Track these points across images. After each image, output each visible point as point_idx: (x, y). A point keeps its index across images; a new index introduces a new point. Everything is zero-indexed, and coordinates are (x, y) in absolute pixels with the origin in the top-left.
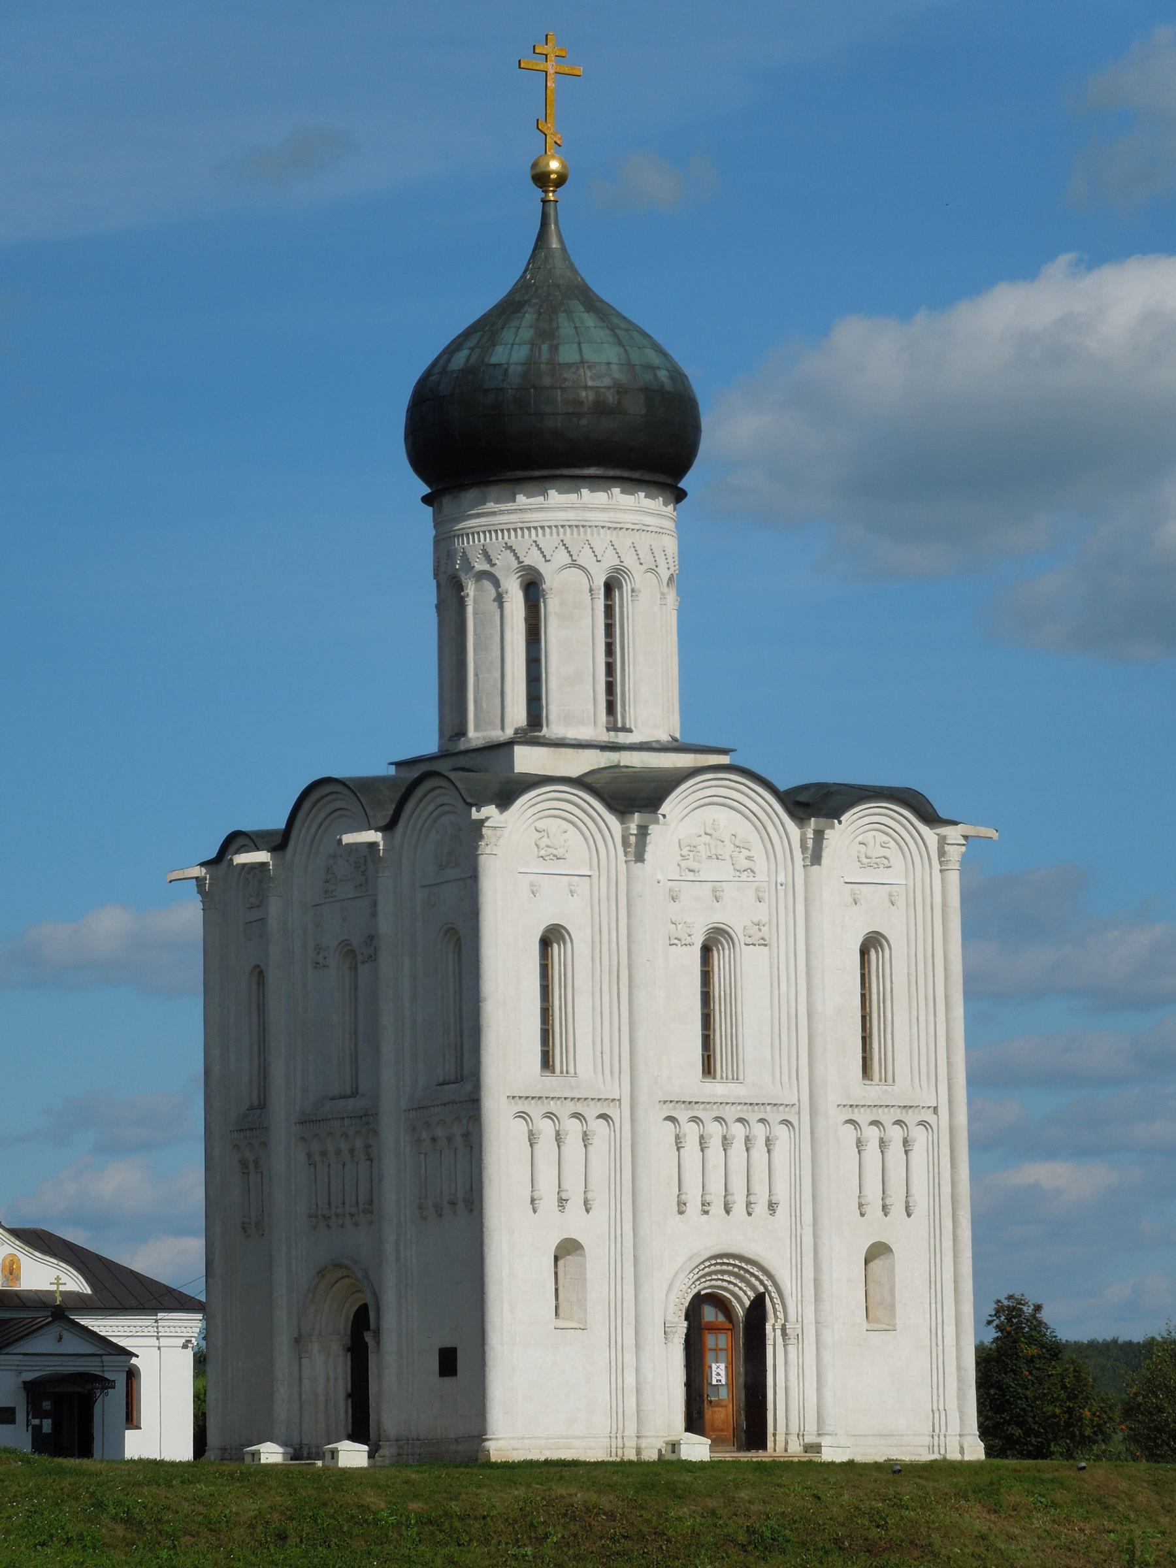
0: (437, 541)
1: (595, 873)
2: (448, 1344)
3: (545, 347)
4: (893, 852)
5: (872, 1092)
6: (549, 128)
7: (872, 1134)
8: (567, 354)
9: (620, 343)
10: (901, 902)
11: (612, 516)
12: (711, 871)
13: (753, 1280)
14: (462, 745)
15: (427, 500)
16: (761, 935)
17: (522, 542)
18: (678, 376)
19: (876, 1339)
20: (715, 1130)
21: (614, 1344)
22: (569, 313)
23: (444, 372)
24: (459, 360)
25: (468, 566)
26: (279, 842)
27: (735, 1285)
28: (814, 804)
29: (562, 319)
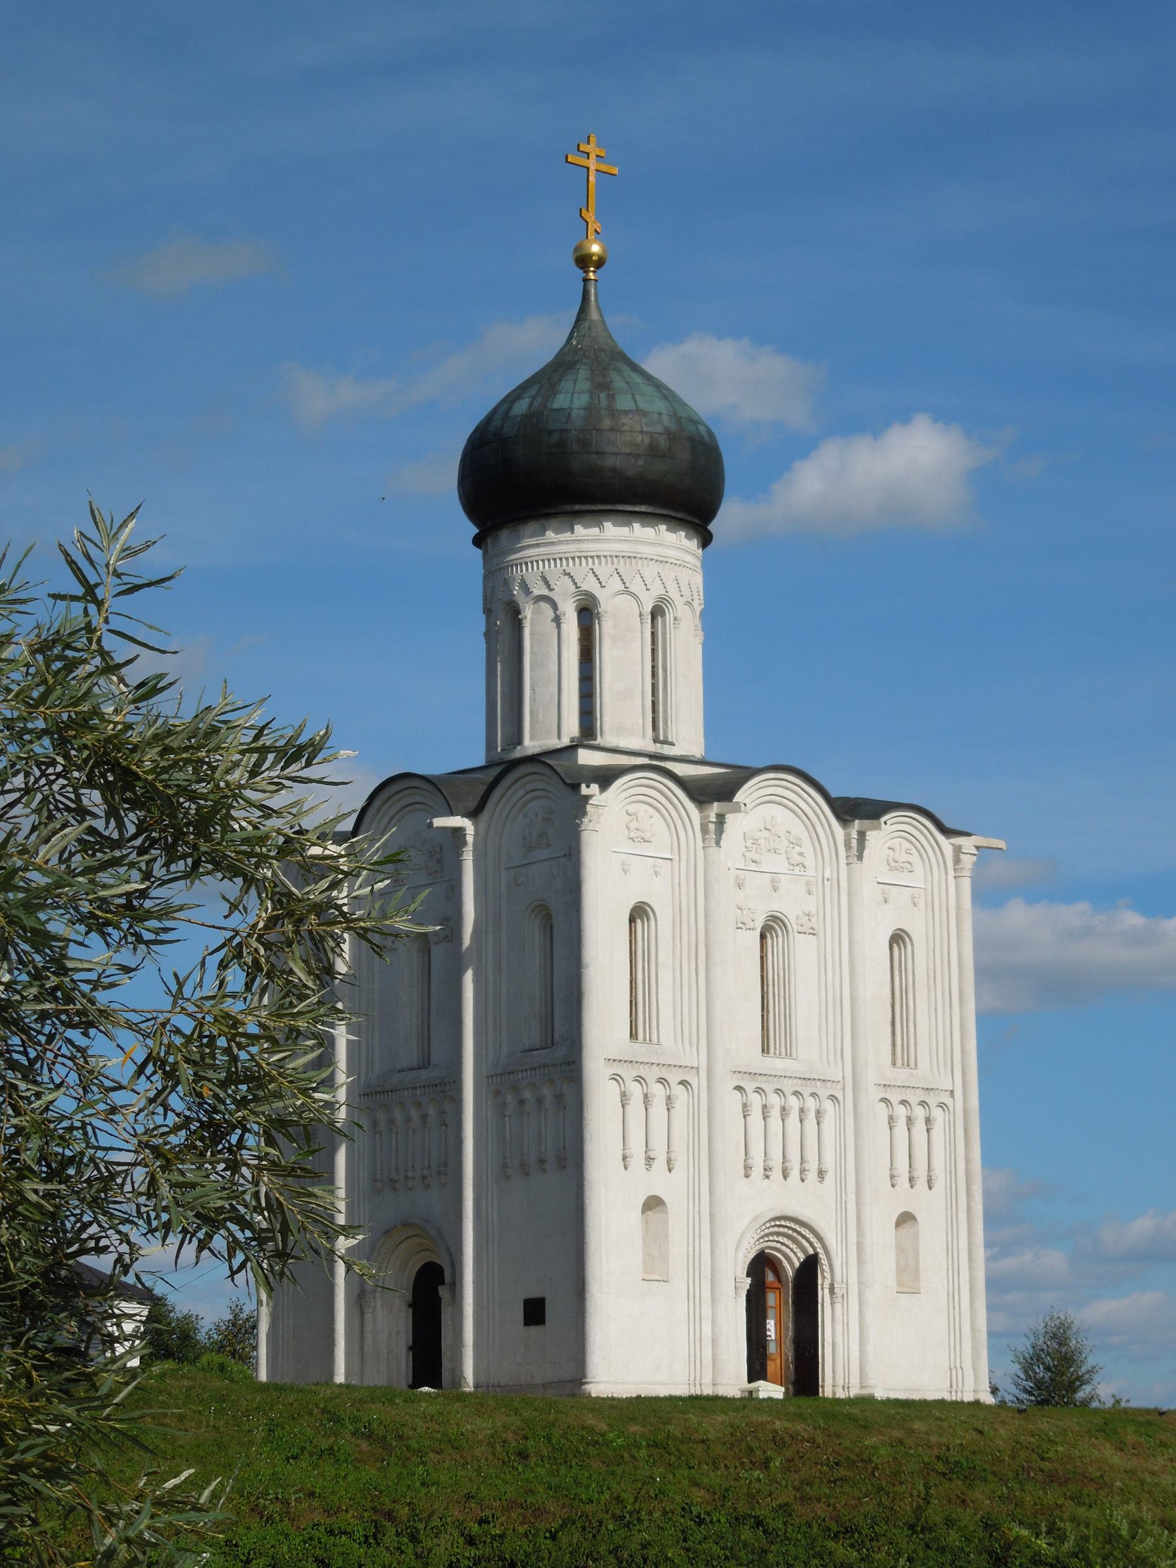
0: (487, 577)
1: (676, 857)
2: (535, 1294)
3: (603, 396)
4: (915, 858)
6: (590, 216)
7: (901, 1112)
9: (666, 398)
10: (922, 904)
11: (659, 550)
12: (770, 863)
13: (804, 1242)
14: (518, 753)
16: (811, 924)
17: (580, 571)
18: (710, 433)
20: (775, 1100)
21: (692, 1297)
22: (619, 371)
23: (506, 416)
24: (521, 407)
25: (526, 590)
27: (787, 1246)
28: (854, 810)
29: (614, 375)
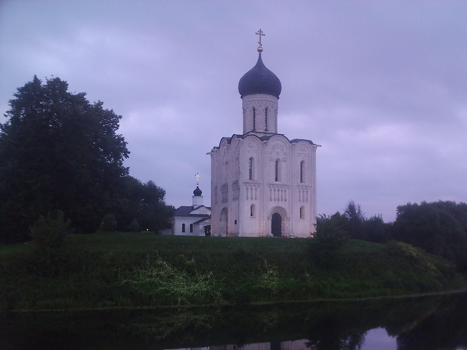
5: (302, 184)
19: (301, 220)
20: (277, 189)
26: (218, 148)
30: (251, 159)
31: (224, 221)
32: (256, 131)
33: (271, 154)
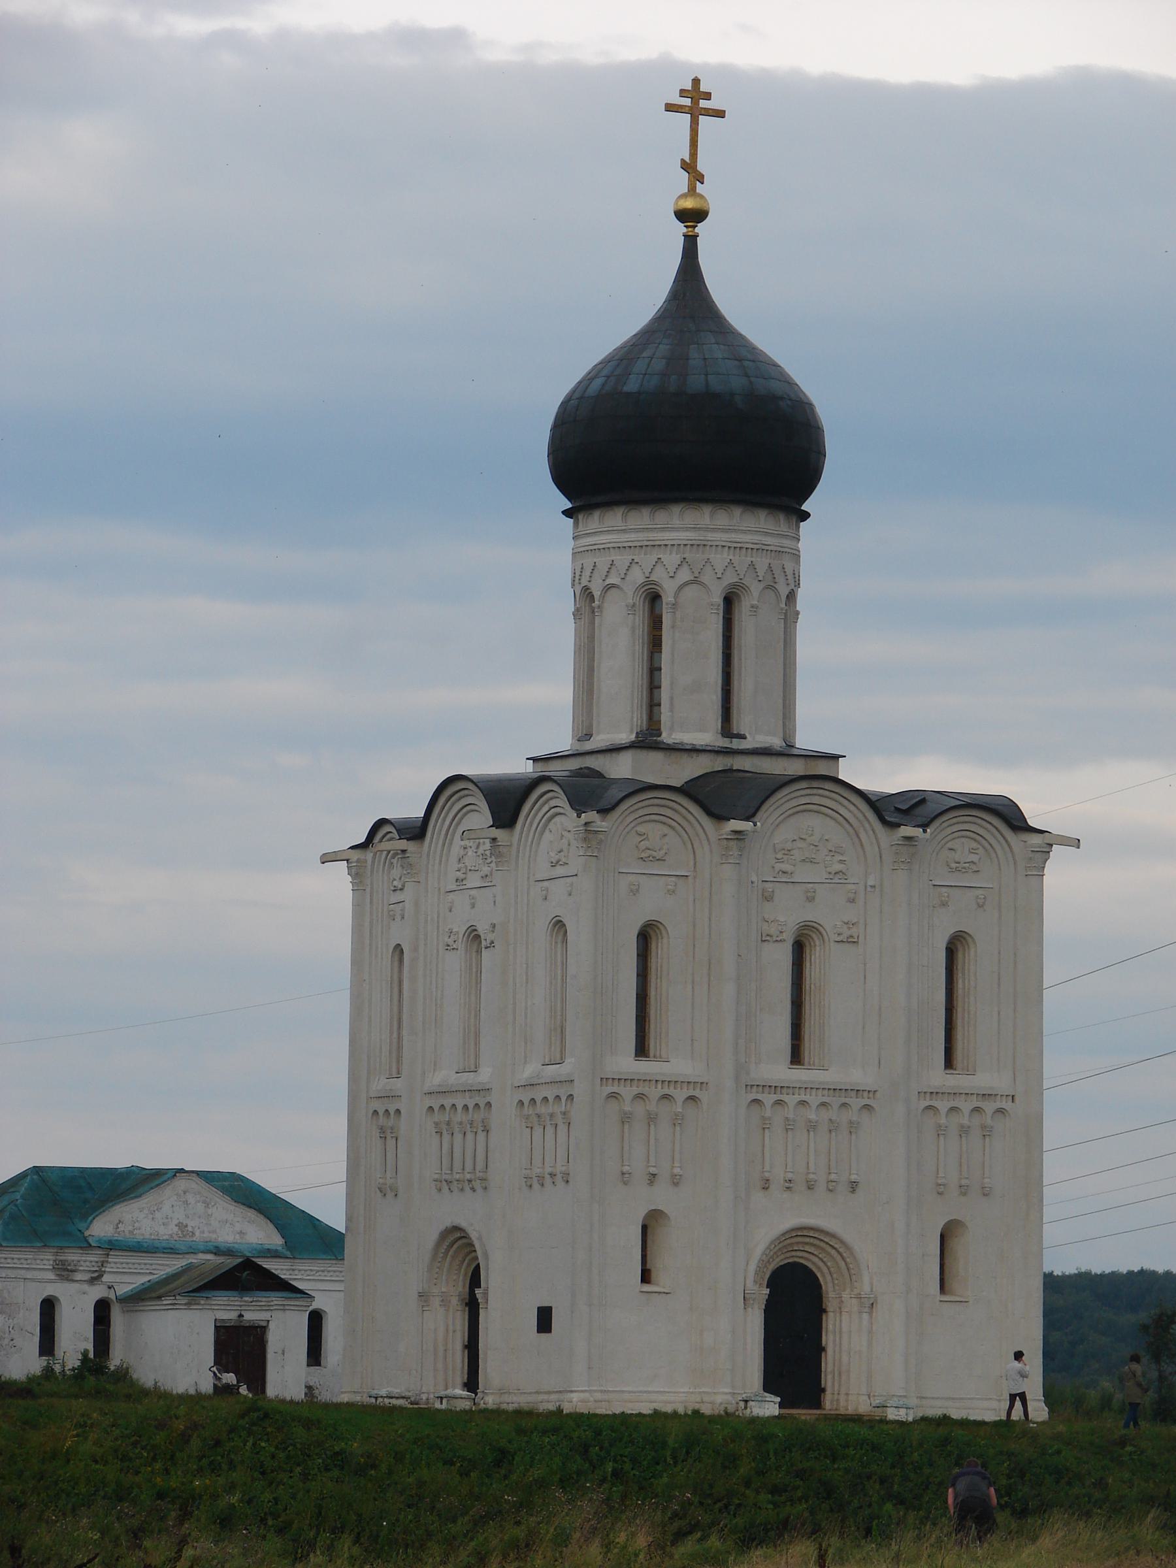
8: (696, 383)
15: (567, 513)
26: (416, 831)
30: (646, 937)
31: (445, 1303)
32: (667, 737)
33: (768, 898)
